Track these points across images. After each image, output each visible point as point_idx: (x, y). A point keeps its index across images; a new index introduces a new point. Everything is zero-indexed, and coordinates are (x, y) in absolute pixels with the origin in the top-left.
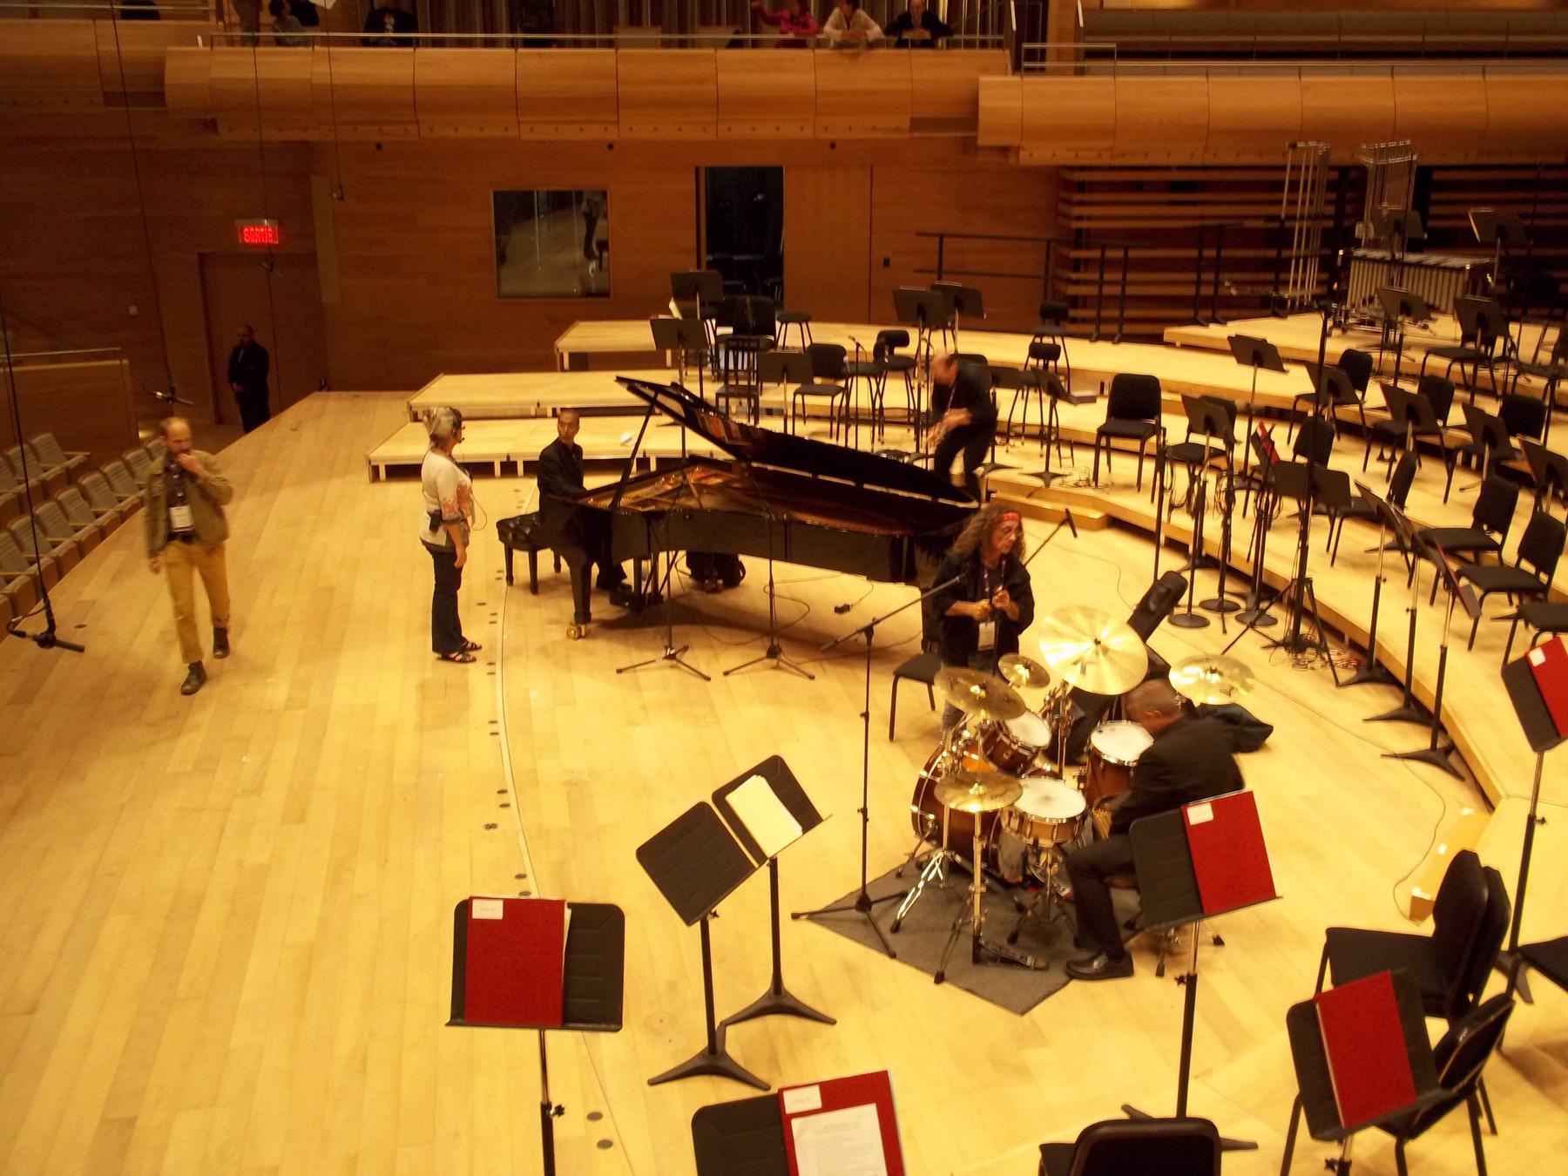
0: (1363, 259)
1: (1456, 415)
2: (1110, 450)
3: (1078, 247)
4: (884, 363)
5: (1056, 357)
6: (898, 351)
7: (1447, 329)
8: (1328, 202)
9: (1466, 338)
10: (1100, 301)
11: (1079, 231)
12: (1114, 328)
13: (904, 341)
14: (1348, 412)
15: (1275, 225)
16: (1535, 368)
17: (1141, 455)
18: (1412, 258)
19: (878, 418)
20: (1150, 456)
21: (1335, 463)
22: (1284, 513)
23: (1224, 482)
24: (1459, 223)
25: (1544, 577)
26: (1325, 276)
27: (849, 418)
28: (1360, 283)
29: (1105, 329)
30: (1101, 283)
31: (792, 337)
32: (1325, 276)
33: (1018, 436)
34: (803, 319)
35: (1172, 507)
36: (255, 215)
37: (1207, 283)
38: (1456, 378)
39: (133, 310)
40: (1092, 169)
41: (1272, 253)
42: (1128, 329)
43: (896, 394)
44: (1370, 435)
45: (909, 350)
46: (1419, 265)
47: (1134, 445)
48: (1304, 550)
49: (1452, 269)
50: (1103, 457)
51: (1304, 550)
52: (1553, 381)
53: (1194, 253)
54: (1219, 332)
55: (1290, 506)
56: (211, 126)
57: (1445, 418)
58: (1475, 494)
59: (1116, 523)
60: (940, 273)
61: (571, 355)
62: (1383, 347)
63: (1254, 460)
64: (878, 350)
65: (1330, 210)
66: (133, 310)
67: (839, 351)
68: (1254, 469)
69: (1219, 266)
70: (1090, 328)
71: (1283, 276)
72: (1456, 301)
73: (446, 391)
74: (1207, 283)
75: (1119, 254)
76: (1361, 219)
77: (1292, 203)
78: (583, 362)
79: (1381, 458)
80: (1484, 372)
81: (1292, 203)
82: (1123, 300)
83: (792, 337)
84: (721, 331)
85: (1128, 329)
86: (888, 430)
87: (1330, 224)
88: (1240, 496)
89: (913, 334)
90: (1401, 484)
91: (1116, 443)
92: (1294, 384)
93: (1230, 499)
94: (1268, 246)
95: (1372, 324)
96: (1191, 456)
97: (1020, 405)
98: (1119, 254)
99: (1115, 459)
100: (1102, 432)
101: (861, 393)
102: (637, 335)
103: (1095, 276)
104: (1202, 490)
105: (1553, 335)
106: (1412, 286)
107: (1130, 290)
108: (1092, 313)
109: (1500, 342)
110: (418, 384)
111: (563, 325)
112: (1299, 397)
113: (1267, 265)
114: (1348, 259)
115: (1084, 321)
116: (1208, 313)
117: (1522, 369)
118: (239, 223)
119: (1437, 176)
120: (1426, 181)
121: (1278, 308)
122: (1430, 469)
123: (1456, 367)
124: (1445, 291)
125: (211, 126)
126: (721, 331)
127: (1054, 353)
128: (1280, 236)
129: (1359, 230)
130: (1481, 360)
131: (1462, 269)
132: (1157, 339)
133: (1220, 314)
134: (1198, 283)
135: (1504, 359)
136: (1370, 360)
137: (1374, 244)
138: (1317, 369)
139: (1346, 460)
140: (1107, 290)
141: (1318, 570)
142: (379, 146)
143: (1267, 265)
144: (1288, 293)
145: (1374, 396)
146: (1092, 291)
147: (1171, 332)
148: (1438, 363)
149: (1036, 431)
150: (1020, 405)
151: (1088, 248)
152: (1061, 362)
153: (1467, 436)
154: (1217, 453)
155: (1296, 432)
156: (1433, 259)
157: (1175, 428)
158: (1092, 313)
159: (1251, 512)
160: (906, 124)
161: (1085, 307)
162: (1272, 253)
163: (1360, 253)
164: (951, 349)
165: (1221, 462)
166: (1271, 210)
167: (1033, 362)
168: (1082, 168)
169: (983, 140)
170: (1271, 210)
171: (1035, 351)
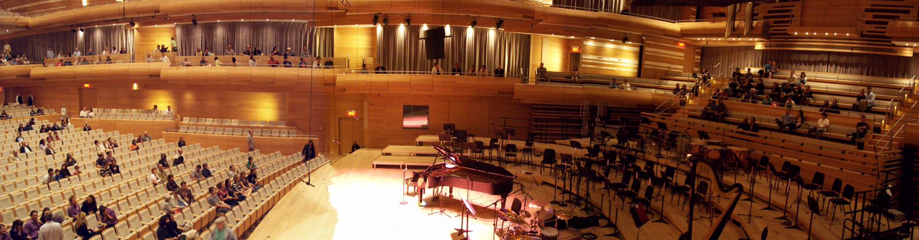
0: (598, 126)
1: (618, 159)
2: (544, 167)
3: (536, 122)
4: (493, 146)
5: (532, 146)
6: (495, 143)
7: (615, 141)
8: (590, 114)
9: (619, 143)
10: (541, 134)
11: (536, 118)
12: (544, 140)
13: (497, 141)
14: (594, 158)
15: (578, 118)
16: (633, 150)
17: (551, 168)
18: (607, 126)
19: (491, 159)
20: (553, 168)
21: (592, 168)
22: (583, 180)
23: (570, 173)
24: (617, 119)
25: (637, 193)
26: (589, 130)
27: (484, 158)
28: (598, 130)
29: (542, 140)
30: (541, 130)
31: (471, 140)
32: (589, 130)
33: (523, 163)
34: (473, 136)
35: (559, 178)
36: (351, 109)
37: (565, 131)
38: (618, 152)
39: (321, 128)
40: (540, 105)
41: (578, 125)
42: (547, 140)
43: (495, 153)
44: (601, 164)
45: (498, 143)
46: (609, 127)
47: (549, 165)
48: (588, 187)
49: (615, 128)
50: (542, 169)
51: (588, 187)
52: (636, 153)
53: (562, 124)
54: (568, 142)
55: (584, 179)
56: (344, 90)
57: (615, 159)
58: (622, 176)
59: (544, 183)
60: (505, 126)
61: (419, 142)
62: (602, 145)
63: (576, 168)
64: (491, 142)
65: (590, 116)
66: (321, 128)
67: (481, 143)
68: (577, 170)
69: (567, 127)
70: (539, 140)
71: (580, 130)
72: (617, 135)
73: (390, 149)
74: (565, 131)
75: (545, 124)
76: (596, 117)
77: (582, 114)
78: (421, 144)
79: (602, 169)
80: (623, 150)
81: (582, 114)
82: (546, 134)
83: (471, 140)
84: (454, 138)
85: (547, 140)
86: (493, 161)
87: (590, 119)
88: (573, 177)
89: (499, 140)
90: (607, 174)
91: (546, 165)
92: (583, 152)
93: (572, 178)
94: (577, 123)
95: (599, 140)
96: (562, 167)
97: (523, 157)
98: (545, 124)
99: (545, 169)
100: (543, 162)
101: (486, 153)
102: (436, 138)
103: (540, 128)
104: (565, 176)
105: (636, 143)
106: (609, 131)
107: (548, 132)
108: (539, 137)
109: (626, 143)
110: (383, 147)
111: (417, 135)
112: (585, 155)
113: (577, 127)
114: (594, 125)
115: (538, 138)
116: (565, 137)
117: (630, 150)
118: (348, 111)
119: (612, 109)
120: (609, 110)
121: (580, 137)
122: (612, 170)
123: (617, 149)
124: (614, 133)
125: (344, 90)
126: (454, 138)
127: (531, 145)
128: (580, 121)
129: (596, 120)
130: (622, 148)
131: (617, 129)
132: (554, 143)
133: (568, 137)
134: (563, 131)
135: (626, 148)
136: (599, 147)
137: (599, 123)
138: (588, 148)
139: (595, 168)
140: (544, 132)
141: (591, 191)
142: (379, 95)
143: (577, 127)
144: (582, 133)
145: (601, 155)
146: (540, 132)
147: (557, 141)
148: (614, 149)
149: (527, 162)
150: (523, 157)
151: (538, 122)
152: (533, 147)
153: (620, 164)
154: (568, 167)
155: (585, 162)
156: (612, 126)
157: (559, 162)
158: (539, 137)
159: (576, 180)
160: (497, 93)
161: (538, 135)
162: (578, 125)
163: (597, 124)
164: (507, 143)
165: (569, 169)
166: (577, 115)
167: (526, 147)
168: (537, 105)
169: (515, 97)
170: (577, 115)
171: (527, 144)
